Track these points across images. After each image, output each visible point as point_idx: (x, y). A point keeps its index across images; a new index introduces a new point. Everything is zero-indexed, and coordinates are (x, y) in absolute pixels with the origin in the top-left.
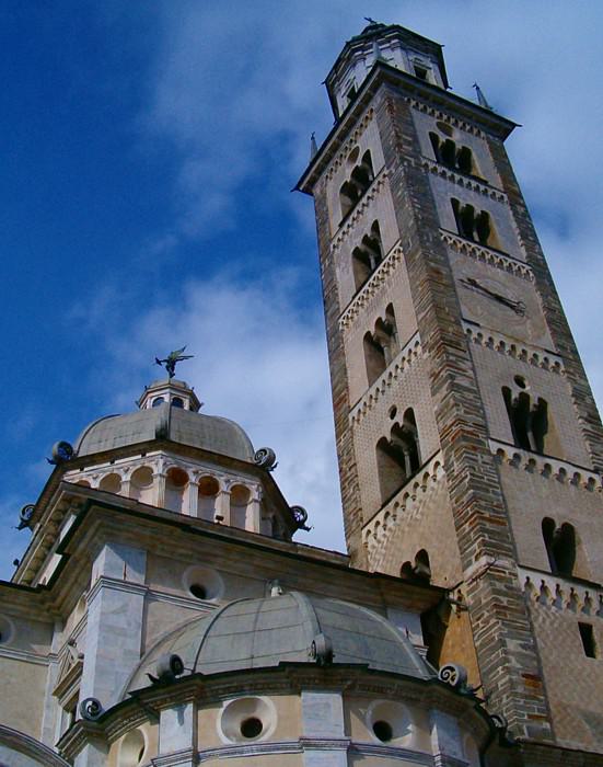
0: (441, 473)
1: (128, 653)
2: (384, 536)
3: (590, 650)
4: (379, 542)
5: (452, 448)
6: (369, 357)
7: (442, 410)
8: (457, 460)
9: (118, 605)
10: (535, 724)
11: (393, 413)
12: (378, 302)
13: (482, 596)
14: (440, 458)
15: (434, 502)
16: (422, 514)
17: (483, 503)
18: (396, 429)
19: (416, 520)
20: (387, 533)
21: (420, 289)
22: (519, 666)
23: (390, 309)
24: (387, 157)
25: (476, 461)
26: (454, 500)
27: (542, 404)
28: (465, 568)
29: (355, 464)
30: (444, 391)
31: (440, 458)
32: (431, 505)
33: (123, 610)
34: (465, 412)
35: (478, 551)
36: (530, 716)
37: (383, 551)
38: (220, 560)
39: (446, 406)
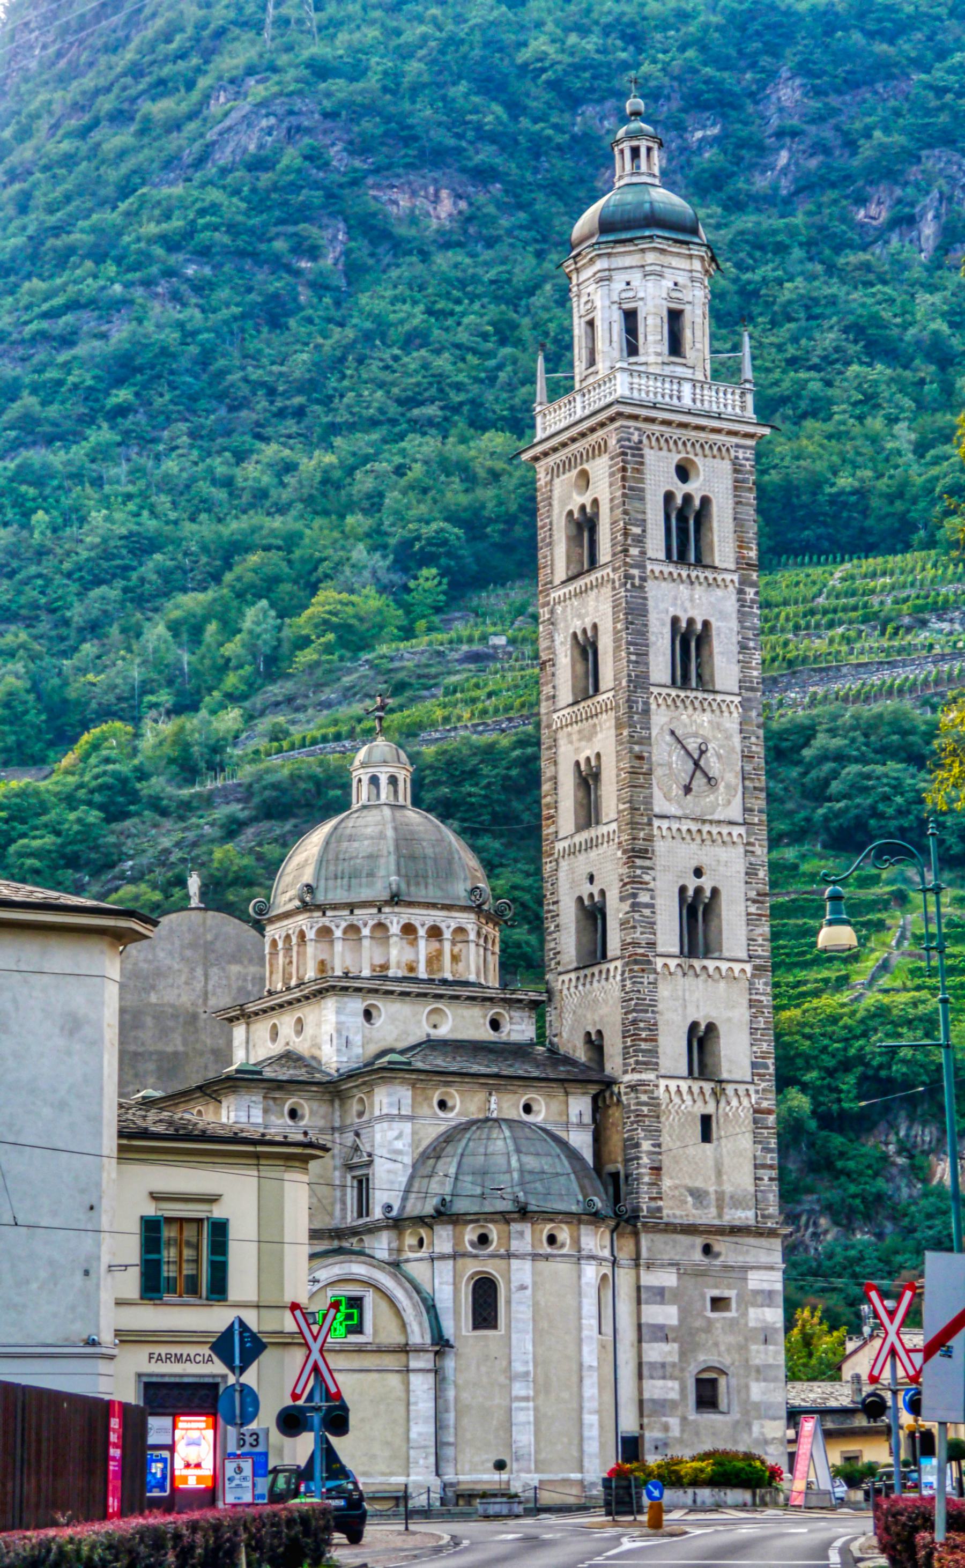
0: (618, 978)
3: (706, 1136)
9: (395, 1133)
10: (653, 1204)
11: (591, 879)
14: (619, 963)
17: (642, 1025)
18: (591, 896)
23: (598, 756)
24: (614, 555)
27: (715, 892)
28: (625, 1072)
30: (626, 906)
36: (651, 1199)
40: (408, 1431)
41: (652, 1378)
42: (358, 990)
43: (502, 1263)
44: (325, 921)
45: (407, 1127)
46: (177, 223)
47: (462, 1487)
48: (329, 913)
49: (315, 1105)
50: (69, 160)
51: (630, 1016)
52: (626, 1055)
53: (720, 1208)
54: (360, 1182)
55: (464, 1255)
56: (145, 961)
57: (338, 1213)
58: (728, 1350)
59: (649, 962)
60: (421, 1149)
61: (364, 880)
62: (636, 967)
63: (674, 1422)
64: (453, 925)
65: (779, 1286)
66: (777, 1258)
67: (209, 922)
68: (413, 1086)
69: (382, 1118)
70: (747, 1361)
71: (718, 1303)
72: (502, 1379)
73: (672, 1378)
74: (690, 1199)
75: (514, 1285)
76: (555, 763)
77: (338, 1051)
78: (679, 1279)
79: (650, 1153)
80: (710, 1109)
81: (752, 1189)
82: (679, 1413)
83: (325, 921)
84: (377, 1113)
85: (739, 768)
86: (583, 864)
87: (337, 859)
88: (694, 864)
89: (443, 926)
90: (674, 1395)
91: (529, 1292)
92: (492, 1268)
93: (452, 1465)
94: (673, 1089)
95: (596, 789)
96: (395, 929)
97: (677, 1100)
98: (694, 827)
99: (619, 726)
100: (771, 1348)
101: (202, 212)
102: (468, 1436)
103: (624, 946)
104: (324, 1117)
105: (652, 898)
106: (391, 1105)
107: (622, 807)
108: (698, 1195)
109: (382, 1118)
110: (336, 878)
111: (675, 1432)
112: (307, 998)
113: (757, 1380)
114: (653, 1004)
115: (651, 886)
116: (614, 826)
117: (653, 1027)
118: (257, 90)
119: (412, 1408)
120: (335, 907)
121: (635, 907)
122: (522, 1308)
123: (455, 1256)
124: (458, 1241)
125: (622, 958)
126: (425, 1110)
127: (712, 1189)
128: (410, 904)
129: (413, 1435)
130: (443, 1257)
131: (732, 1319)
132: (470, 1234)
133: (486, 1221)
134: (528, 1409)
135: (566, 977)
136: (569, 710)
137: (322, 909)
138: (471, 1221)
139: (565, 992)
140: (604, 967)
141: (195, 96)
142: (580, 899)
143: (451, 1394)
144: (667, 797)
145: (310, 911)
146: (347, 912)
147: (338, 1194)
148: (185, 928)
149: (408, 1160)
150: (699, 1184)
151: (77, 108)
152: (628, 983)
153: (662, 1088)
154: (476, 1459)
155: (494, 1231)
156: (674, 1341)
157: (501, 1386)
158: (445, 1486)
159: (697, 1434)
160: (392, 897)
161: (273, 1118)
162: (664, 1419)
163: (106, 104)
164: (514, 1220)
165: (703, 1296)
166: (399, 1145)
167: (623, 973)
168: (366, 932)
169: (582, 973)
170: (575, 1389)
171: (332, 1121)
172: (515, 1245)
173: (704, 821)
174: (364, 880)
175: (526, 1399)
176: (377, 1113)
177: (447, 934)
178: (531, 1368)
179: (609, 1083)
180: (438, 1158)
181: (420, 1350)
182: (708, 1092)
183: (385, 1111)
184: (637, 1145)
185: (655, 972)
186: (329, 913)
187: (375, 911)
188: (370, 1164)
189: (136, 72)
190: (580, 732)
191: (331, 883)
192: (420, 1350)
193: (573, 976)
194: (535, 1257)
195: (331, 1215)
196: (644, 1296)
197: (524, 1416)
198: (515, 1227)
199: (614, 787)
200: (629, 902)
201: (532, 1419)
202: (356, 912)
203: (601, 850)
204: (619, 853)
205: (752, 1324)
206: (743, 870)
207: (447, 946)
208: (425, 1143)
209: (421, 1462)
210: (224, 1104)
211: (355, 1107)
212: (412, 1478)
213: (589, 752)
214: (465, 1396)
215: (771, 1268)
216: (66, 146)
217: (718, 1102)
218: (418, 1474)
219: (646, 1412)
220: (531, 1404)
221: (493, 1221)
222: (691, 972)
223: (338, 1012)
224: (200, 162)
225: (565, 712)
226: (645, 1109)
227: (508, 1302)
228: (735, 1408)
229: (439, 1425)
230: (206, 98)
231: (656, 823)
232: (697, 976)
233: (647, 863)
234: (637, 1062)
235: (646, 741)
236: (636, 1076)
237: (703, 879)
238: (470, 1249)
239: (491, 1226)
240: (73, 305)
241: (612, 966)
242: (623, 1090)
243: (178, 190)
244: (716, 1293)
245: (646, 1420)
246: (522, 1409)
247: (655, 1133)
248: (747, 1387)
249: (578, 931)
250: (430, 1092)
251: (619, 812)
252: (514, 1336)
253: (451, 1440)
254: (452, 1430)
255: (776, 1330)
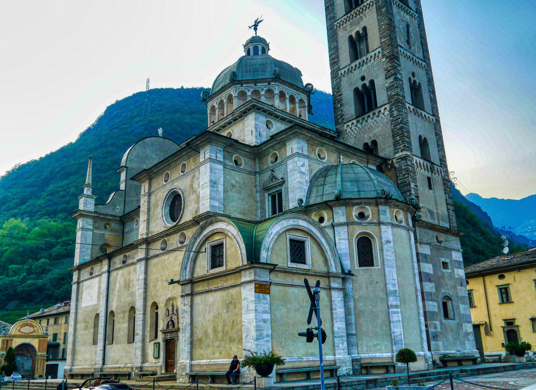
0: (387, 113)
1: (306, 181)
2: (355, 129)
3: (430, 188)
4: (352, 131)
5: (394, 104)
6: (350, 47)
7: (390, 87)
8: (396, 110)
9: (301, 163)
11: (363, 78)
12: (358, 23)
13: (403, 165)
15: (382, 123)
16: (376, 126)
17: (405, 130)
18: (364, 86)
19: (372, 127)
20: (357, 128)
21: (383, 27)
22: (414, 193)
23: (365, 29)
25: (403, 112)
26: (393, 126)
28: (395, 153)
29: (341, 95)
30: (391, 79)
31: (387, 106)
32: (380, 124)
33: (303, 166)
34: (400, 91)
35: (402, 148)
37: (355, 135)
38: (326, 146)
39: (393, 86)
40: (333, 326)
41: (428, 300)
42: (264, 111)
43: (376, 228)
44: (243, 89)
45: (306, 162)
46: (126, 141)
47: (363, 362)
48: (244, 85)
49: (247, 160)
50: (108, 134)
51: (398, 127)
52: (396, 144)
53: (438, 220)
54: (273, 198)
55: (353, 223)
56: (142, 152)
57: (259, 214)
58: (451, 288)
59: (404, 104)
60: (312, 175)
61: (260, 73)
62: (400, 104)
63: (438, 323)
64: (299, 98)
65: (461, 259)
66: (459, 246)
67: (166, 143)
68: (308, 141)
69: (292, 156)
70: (457, 293)
71: (445, 265)
72: (382, 295)
73: (435, 301)
74: (428, 214)
75: (384, 240)
76: (337, 42)
77: (256, 137)
78: (431, 250)
79: (414, 188)
80: (430, 175)
81: (447, 214)
82: (439, 319)
83: (243, 89)
84: (289, 153)
85: (420, 40)
86: (357, 74)
87: (246, 65)
88: (412, 70)
89: (296, 96)
90: (436, 310)
91: (392, 244)
92: (370, 230)
93: (355, 348)
94: (418, 162)
95: (360, 47)
96: (277, 92)
97: (419, 168)
98: (411, 56)
99: (378, 9)
100: (463, 288)
101: (131, 140)
102: (364, 329)
103: (390, 97)
104: (251, 166)
105: (402, 77)
106: (299, 148)
107: (383, 40)
108: (431, 213)
109: (292, 156)
110: (247, 72)
111: (439, 329)
112: (235, 120)
113: (461, 303)
114: (406, 123)
115: (401, 72)
116: (380, 49)
117: (408, 132)
118: (141, 123)
119: (334, 311)
120: (248, 82)
121: (396, 79)
122: (389, 253)
123: (347, 224)
124: (349, 215)
125: (389, 103)
126: (312, 156)
127: (435, 211)
128: (284, 82)
129: (336, 329)
130: (340, 225)
131: (450, 273)
132: (355, 211)
133: (366, 204)
134: (397, 313)
135: (350, 124)
136: (345, 17)
137: (241, 83)
138: (357, 204)
139: (348, 130)
140: (377, 111)
141: (130, 125)
142: (356, 90)
143: (352, 304)
144: (400, 40)
145: (236, 84)
146: (253, 85)
147: (259, 204)
148: (157, 143)
149: (308, 178)
150: (430, 208)
151: (110, 127)
152: (395, 113)
153: (415, 161)
154: (370, 344)
155: (369, 211)
156: (433, 282)
157: (382, 299)
158: (353, 361)
159: (446, 330)
160: (277, 77)
161: (227, 161)
162: (434, 322)
163: (115, 126)
164: (382, 204)
165: (440, 261)
166: (303, 169)
167: (391, 109)
168: (263, 93)
169: (360, 118)
170: (415, 302)
171: (255, 169)
172: (382, 218)
173: (414, 55)
174: (260, 73)
175: (396, 306)
176: (289, 153)
177: (297, 101)
178: (397, 289)
179: (385, 160)
180: (325, 177)
181: (336, 276)
182: (429, 167)
183: (295, 151)
184: (409, 184)
185: (406, 109)
186: (244, 85)
187: (267, 84)
188: (283, 182)
189: (120, 122)
190: (351, 24)
191: (244, 74)
192: (336, 276)
193: (355, 121)
194: (393, 225)
195: (256, 215)
196: (420, 258)
197: (396, 317)
198: (381, 208)
199: (378, 35)
200: (393, 77)
201: (400, 319)
202: (257, 84)
203: (369, 64)
204: (384, 60)
205: (456, 276)
206: (427, 80)
207: (297, 106)
208: (314, 172)
209: (341, 346)
210: (202, 152)
211: (270, 159)
212: (337, 356)
213: (359, 28)
214: (360, 304)
215: (458, 251)
216: (108, 132)
217: (432, 172)
218: (339, 354)
219: (428, 319)
220: (399, 310)
221: (369, 204)
222: (417, 114)
223: (256, 119)
224: (130, 133)
225: (342, 19)
226: (410, 168)
227: (382, 250)
228: (457, 317)
229: (348, 324)
230: (132, 125)
231: (400, 48)
232: (419, 116)
233: (398, 62)
234: (405, 146)
235: (392, 14)
236: (405, 153)
237: (415, 78)
238: (356, 220)
239: (367, 207)
240: (107, 153)
241: (382, 109)
242: (395, 161)
243: (127, 137)
244: (443, 260)
245: (428, 322)
246: (395, 313)
247: (415, 180)
248: (459, 307)
249: (355, 104)
250: (315, 147)
251: (381, 43)
252: (387, 269)
253: (354, 332)
254: (354, 327)
255: (463, 279)
